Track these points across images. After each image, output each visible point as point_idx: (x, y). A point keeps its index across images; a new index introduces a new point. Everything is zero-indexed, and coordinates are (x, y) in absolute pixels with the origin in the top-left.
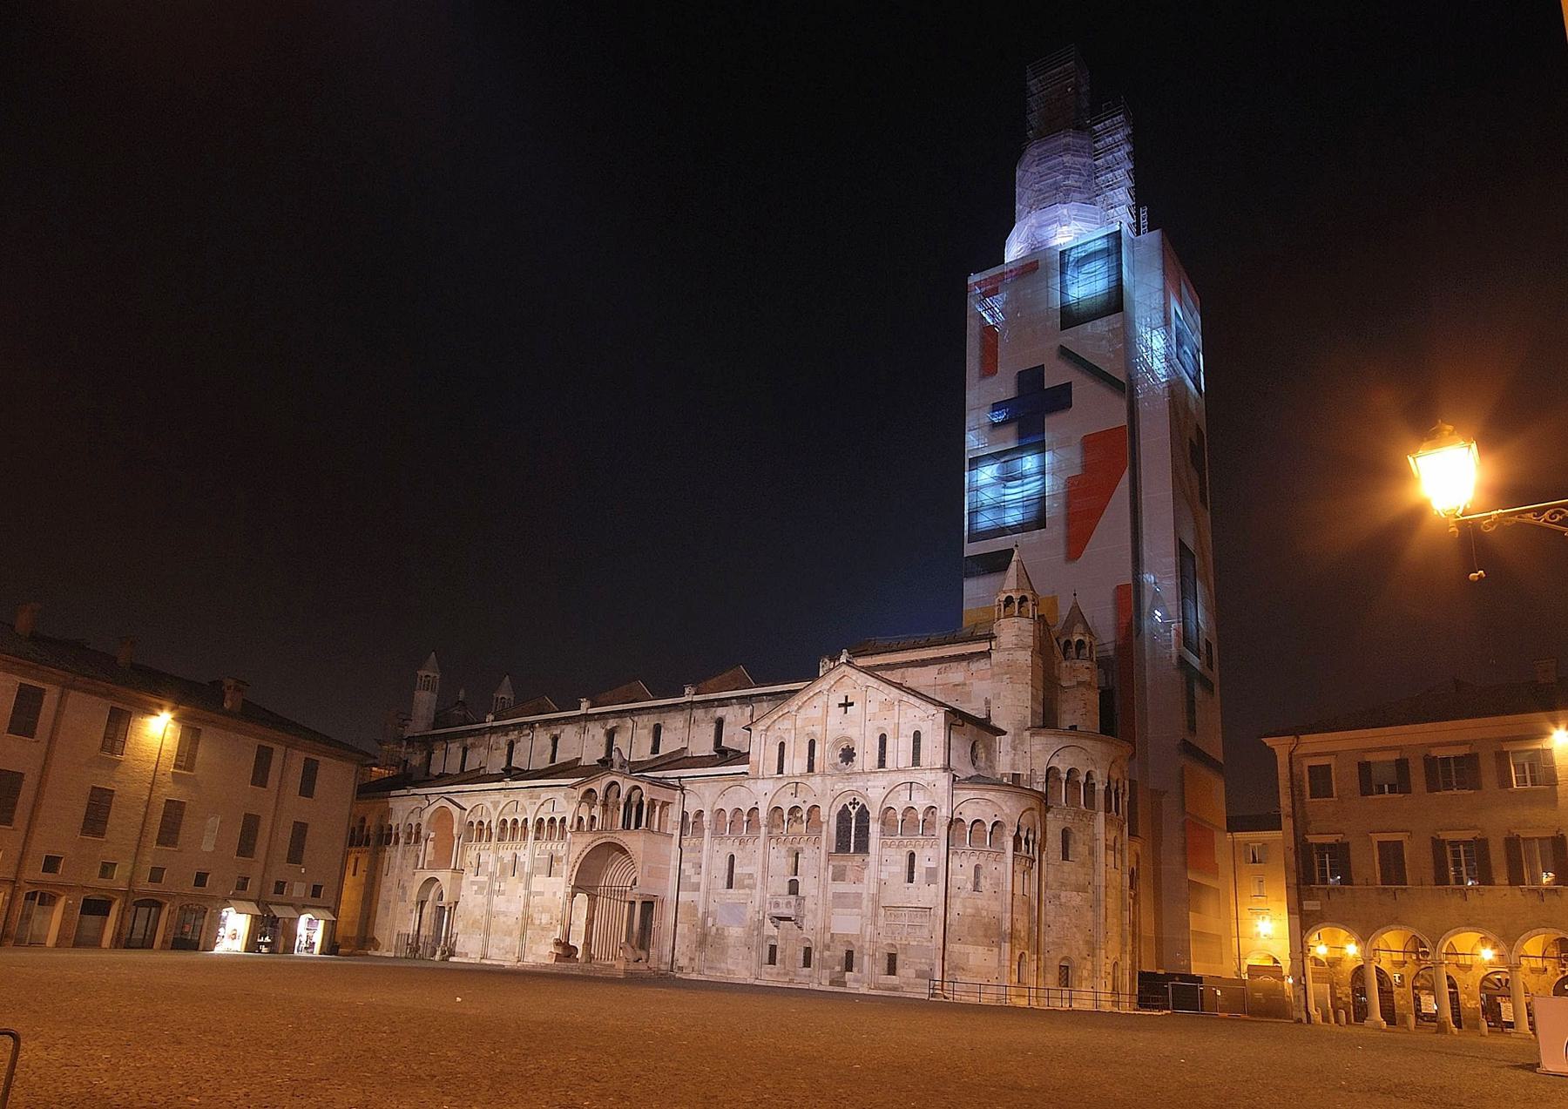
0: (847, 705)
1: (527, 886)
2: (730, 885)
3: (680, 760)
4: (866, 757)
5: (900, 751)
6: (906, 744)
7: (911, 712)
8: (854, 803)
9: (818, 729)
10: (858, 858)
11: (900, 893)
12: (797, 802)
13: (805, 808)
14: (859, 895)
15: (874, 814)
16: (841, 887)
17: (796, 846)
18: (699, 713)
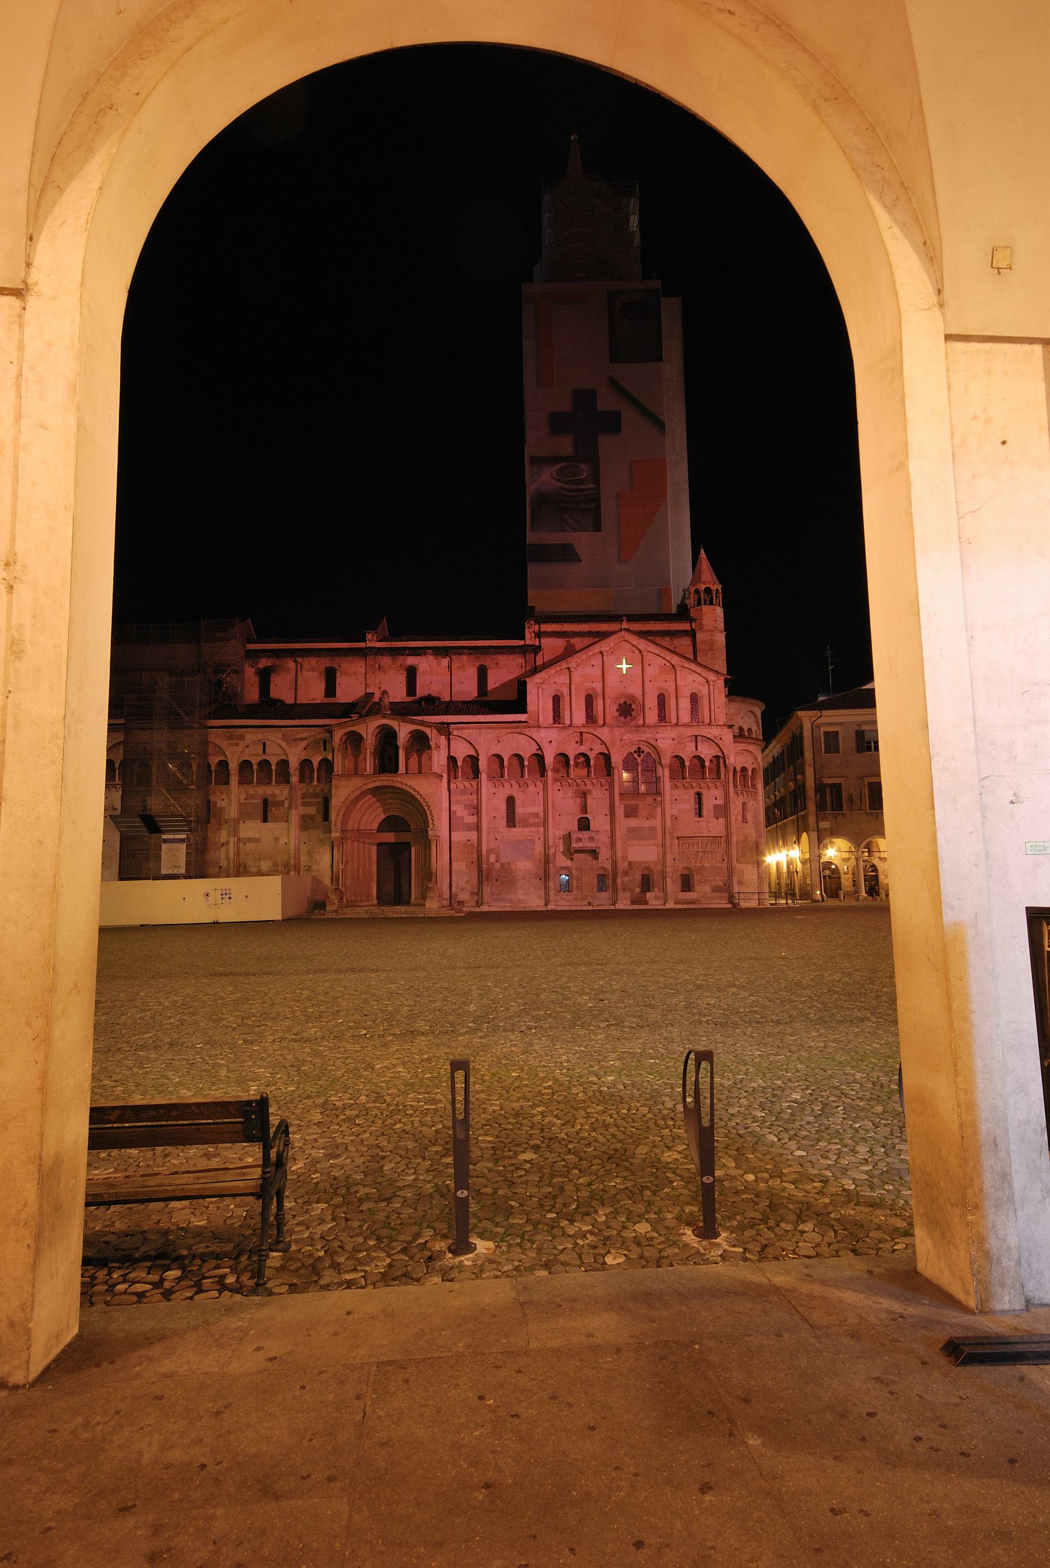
3: (431, 704)
6: (685, 704)
8: (639, 751)
9: (598, 686)
11: (690, 825)
12: (583, 749)
14: (653, 829)
15: (666, 760)
16: (634, 823)
17: (583, 788)
18: (385, 660)
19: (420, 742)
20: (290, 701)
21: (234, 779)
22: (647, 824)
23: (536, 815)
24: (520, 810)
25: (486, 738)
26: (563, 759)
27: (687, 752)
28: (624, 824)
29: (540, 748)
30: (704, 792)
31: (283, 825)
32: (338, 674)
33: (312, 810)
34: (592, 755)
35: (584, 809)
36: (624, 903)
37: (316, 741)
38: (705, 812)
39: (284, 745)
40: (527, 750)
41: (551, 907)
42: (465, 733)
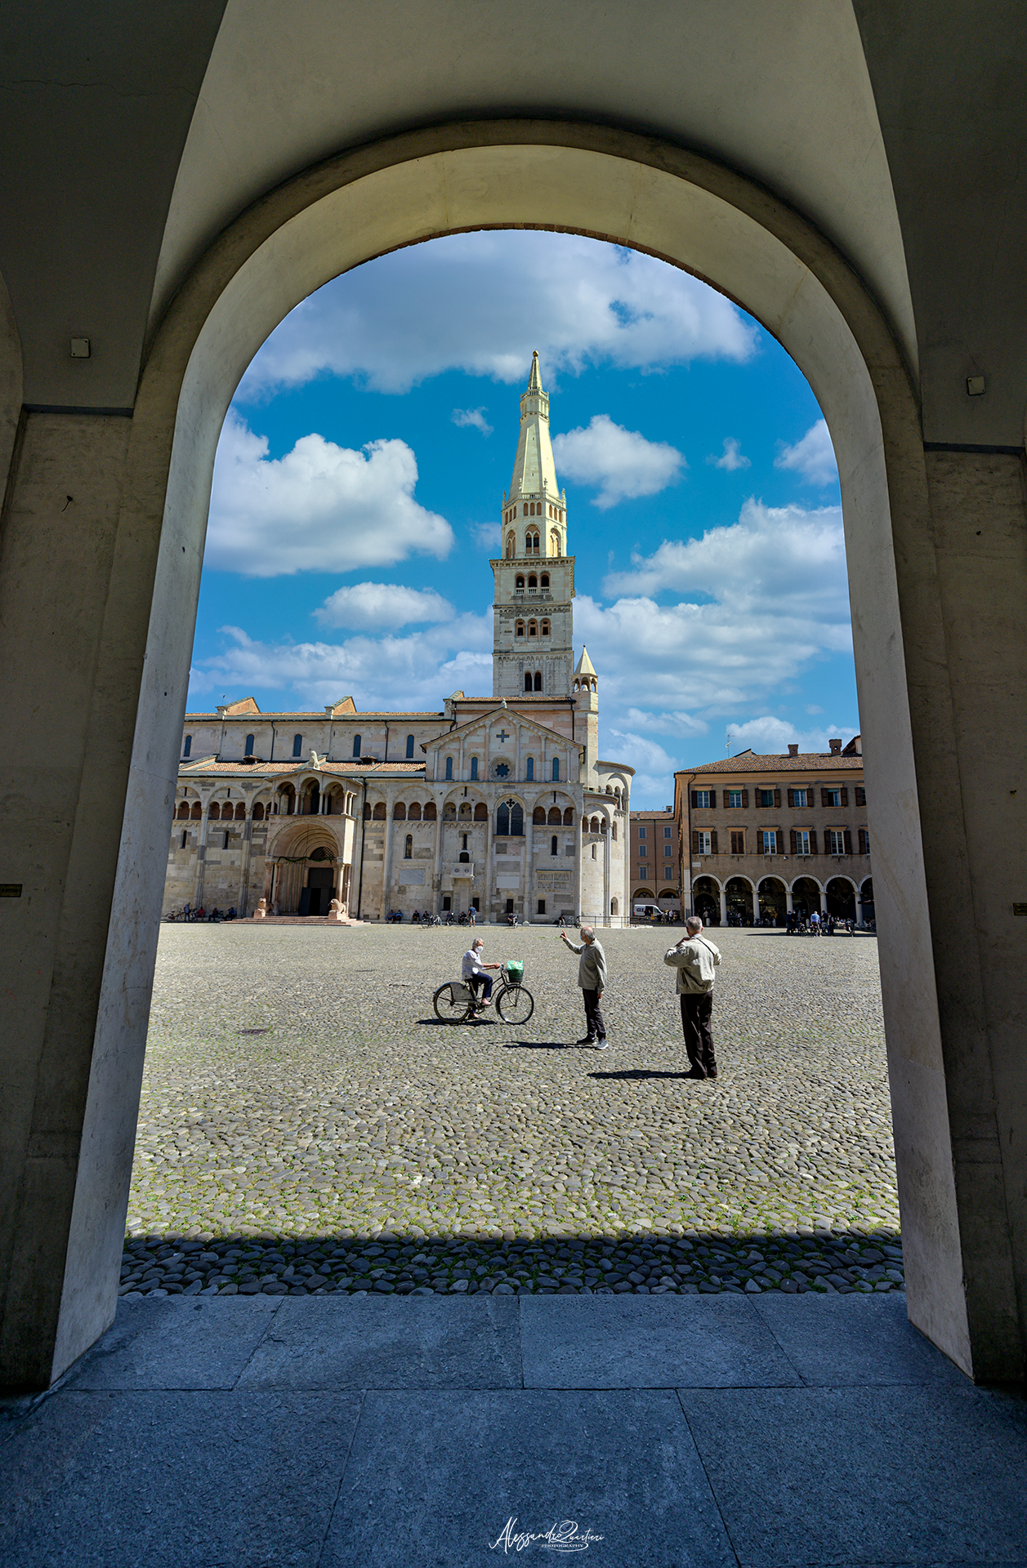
0: (503, 736)
1: (202, 856)
2: (408, 856)
4: (519, 772)
5: (543, 770)
7: (553, 746)
8: (511, 802)
9: (481, 751)
10: (516, 839)
12: (467, 800)
13: (473, 805)
14: (518, 864)
16: (503, 858)
21: (204, 816)
22: (512, 859)
24: (416, 846)
27: (547, 804)
30: (559, 836)
35: (465, 847)
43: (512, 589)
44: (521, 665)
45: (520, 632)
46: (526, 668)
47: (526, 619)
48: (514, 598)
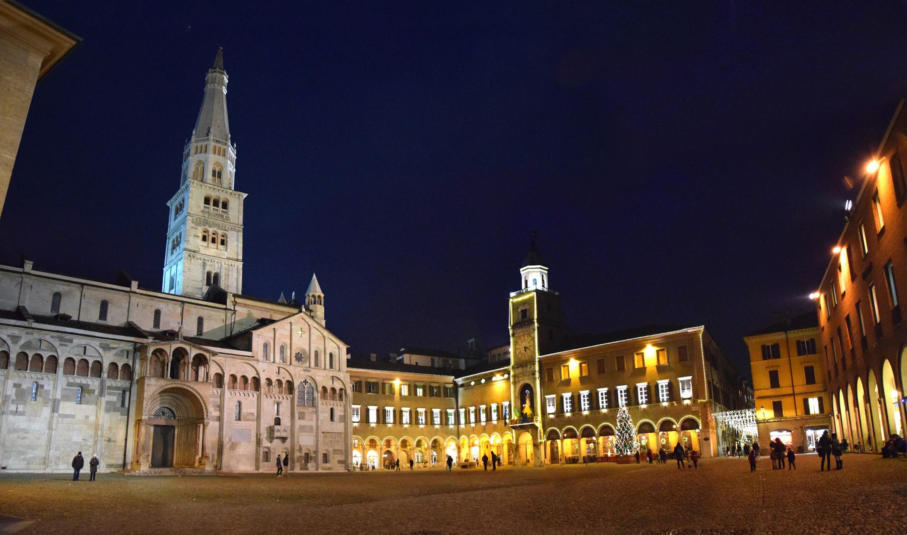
1: (55, 409)
8: (306, 382)
14: (311, 427)
17: (277, 399)
19: (201, 360)
20: (75, 318)
21: (60, 370)
23: (253, 414)
25: (229, 362)
26: (269, 381)
27: (329, 386)
28: (298, 423)
29: (258, 374)
30: (335, 407)
31: (93, 407)
32: (109, 305)
33: (114, 398)
34: (284, 381)
36: (297, 470)
37: (122, 351)
38: (336, 417)
39: (101, 350)
40: (250, 375)
41: (261, 471)
42: (216, 358)
43: (202, 204)
44: (204, 265)
45: (204, 239)
46: (207, 269)
47: (211, 230)
48: (203, 211)
